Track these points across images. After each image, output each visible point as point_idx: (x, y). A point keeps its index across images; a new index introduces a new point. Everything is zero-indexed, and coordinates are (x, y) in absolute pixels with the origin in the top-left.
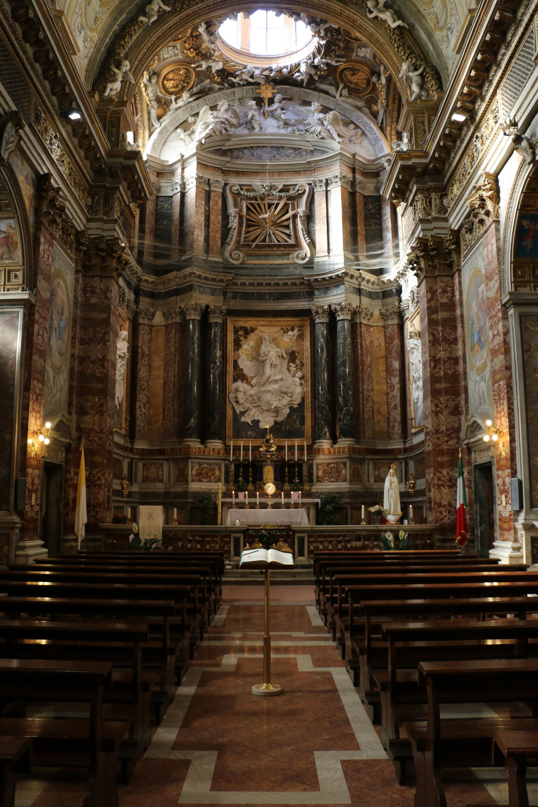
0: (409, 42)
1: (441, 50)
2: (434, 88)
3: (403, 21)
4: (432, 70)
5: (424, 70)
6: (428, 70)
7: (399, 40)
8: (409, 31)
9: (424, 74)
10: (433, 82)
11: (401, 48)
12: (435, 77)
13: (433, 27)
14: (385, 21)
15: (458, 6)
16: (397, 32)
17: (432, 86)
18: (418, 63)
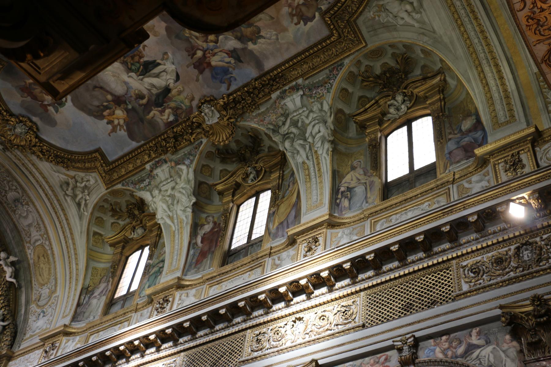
0: (11, 296)
1: (29, 318)
2: (7, 343)
3: (17, 281)
4: (14, 328)
5: (8, 325)
6: (11, 326)
7: (5, 291)
8: (16, 289)
9: (7, 327)
10: (9, 338)
11: (3, 298)
12: (13, 334)
13: (33, 299)
14: (5, 272)
15: (58, 304)
16: (7, 284)
17: (6, 340)
18: (8, 317)
